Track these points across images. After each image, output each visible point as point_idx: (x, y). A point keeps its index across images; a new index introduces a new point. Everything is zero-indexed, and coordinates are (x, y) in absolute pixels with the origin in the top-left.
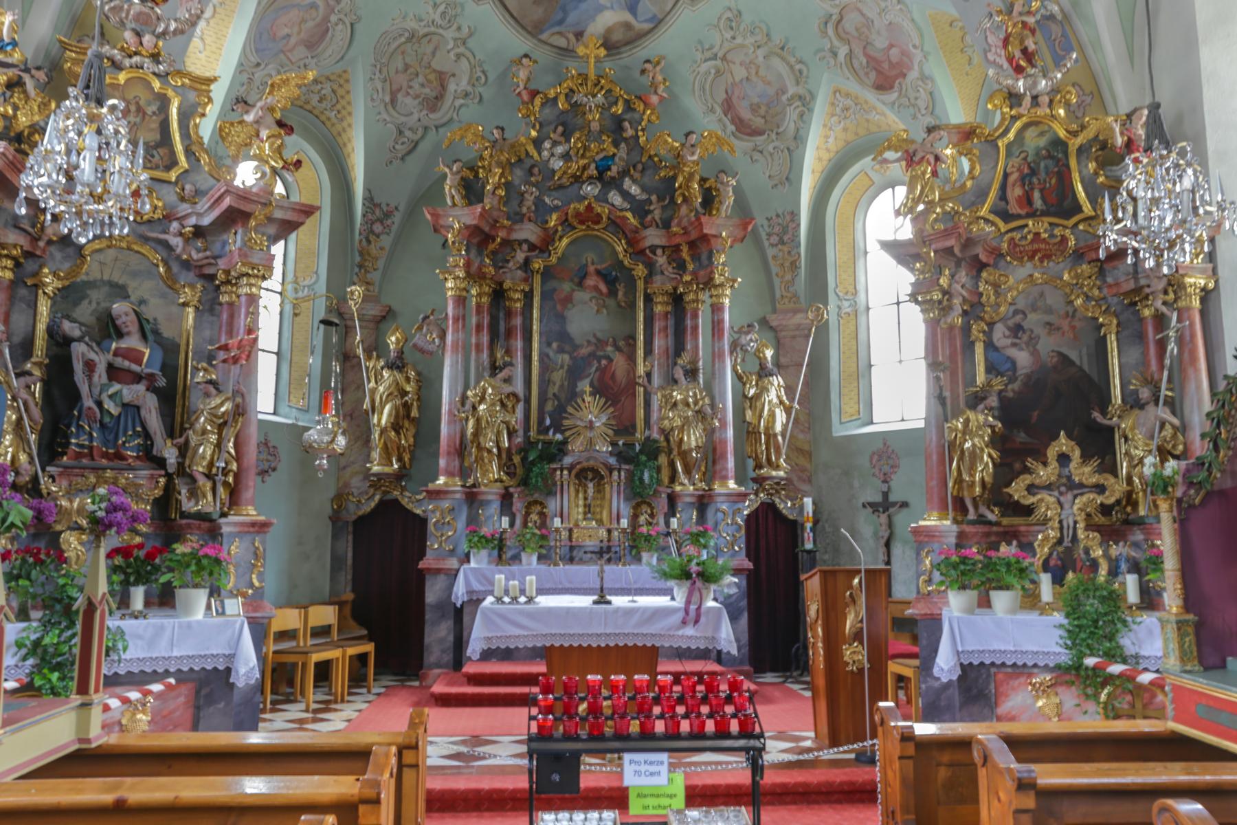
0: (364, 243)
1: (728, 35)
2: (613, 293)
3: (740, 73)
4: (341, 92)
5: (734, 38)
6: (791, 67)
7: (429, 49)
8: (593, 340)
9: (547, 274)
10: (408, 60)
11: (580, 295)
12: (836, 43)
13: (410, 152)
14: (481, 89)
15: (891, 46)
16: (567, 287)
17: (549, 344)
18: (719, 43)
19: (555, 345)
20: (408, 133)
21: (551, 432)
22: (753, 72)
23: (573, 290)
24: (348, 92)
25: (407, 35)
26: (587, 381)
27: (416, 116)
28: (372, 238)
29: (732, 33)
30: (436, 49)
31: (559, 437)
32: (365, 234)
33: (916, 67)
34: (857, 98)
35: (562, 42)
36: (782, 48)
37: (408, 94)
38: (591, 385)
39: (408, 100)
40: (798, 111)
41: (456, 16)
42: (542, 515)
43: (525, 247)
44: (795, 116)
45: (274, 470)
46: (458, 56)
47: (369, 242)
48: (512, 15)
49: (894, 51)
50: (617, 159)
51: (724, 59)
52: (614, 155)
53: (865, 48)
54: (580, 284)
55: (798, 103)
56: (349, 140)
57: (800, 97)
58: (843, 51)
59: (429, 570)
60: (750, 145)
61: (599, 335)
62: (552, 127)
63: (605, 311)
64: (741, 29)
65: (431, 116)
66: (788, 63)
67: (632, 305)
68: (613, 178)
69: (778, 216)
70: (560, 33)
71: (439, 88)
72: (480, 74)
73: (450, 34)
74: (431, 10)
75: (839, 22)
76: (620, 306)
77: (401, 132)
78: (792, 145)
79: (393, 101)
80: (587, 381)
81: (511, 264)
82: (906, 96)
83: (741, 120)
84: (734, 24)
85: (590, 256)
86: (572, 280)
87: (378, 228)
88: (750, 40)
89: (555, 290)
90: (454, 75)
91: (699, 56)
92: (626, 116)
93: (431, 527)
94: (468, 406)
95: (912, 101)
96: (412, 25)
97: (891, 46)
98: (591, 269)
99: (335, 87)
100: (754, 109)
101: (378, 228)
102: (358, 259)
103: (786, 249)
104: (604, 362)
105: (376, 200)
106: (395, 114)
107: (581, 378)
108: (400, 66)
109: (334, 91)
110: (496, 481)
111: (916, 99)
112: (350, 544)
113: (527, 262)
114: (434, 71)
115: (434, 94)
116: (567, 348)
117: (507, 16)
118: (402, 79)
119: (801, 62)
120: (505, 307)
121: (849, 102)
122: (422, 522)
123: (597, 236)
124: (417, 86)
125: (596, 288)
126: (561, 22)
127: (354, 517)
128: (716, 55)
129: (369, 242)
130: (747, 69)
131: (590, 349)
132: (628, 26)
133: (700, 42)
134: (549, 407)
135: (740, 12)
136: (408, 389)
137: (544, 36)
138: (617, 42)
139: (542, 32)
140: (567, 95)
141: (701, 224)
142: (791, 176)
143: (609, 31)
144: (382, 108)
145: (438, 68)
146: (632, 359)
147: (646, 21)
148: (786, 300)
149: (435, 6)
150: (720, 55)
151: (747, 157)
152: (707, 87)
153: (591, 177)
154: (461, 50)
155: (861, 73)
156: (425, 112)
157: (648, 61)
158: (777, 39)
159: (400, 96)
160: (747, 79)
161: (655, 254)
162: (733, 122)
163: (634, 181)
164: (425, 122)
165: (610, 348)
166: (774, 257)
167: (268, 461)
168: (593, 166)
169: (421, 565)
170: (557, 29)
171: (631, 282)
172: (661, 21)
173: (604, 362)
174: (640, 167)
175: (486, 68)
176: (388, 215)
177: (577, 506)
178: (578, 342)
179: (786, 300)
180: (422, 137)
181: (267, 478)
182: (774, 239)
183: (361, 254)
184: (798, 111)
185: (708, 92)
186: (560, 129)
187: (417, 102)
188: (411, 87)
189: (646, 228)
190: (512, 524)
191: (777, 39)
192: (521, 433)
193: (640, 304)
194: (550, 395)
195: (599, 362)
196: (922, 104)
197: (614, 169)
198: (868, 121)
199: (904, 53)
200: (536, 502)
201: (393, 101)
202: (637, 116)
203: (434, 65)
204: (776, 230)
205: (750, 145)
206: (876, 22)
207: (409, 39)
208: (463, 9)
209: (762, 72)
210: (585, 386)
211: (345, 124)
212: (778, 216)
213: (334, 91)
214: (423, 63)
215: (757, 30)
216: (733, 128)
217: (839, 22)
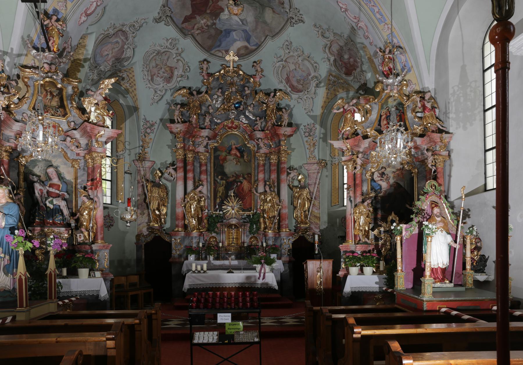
0: (143, 137)
1: (287, 51)
2: (242, 156)
3: (292, 67)
4: (131, 76)
5: (289, 53)
6: (312, 65)
7: (166, 58)
8: (235, 175)
9: (216, 149)
10: (157, 62)
11: (229, 157)
13: (160, 100)
14: (188, 74)
16: (224, 154)
17: (218, 177)
18: (284, 54)
19: (220, 177)
20: (159, 92)
23: (227, 155)
24: (134, 76)
25: (156, 52)
27: (162, 85)
39: (158, 79)
40: (315, 82)
43: (207, 139)
44: (314, 85)
46: (178, 60)
47: (145, 136)
50: (242, 103)
51: (286, 61)
57: (316, 77)
60: (297, 96)
61: (237, 173)
62: (217, 90)
64: (292, 49)
65: (168, 85)
68: (241, 111)
69: (308, 125)
70: (218, 50)
72: (187, 67)
73: (174, 51)
76: (245, 162)
77: (156, 92)
78: (313, 96)
79: (152, 79)
83: (293, 86)
87: (148, 131)
88: (296, 54)
89: (219, 155)
90: (176, 68)
91: (275, 60)
92: (247, 85)
96: (159, 48)
98: (234, 147)
99: (128, 74)
100: (298, 81)
101: (148, 131)
102: (141, 143)
104: (239, 183)
105: (148, 120)
106: (153, 85)
108: (154, 65)
109: (128, 76)
116: (225, 178)
117: (197, 44)
118: (155, 70)
120: (200, 162)
123: (236, 134)
125: (236, 155)
128: (282, 59)
129: (145, 136)
133: (276, 54)
138: (242, 54)
140: (222, 77)
141: (275, 130)
143: (239, 50)
145: (170, 66)
147: (254, 45)
149: (167, 40)
151: (296, 101)
152: (279, 72)
154: (179, 58)
157: (255, 62)
162: (290, 87)
163: (250, 112)
164: (166, 87)
165: (241, 178)
166: (307, 141)
168: (233, 106)
172: (260, 45)
173: (239, 183)
174: (252, 106)
175: (189, 65)
176: (152, 125)
178: (229, 176)
179: (311, 159)
180: (165, 94)
182: (307, 134)
183: (142, 141)
184: (315, 82)
185: (280, 75)
187: (162, 79)
189: (255, 131)
197: (242, 107)
201: (152, 79)
202: (251, 85)
205: (297, 96)
207: (157, 54)
208: (179, 41)
209: (301, 67)
212: (308, 125)
213: (128, 76)
216: (290, 89)
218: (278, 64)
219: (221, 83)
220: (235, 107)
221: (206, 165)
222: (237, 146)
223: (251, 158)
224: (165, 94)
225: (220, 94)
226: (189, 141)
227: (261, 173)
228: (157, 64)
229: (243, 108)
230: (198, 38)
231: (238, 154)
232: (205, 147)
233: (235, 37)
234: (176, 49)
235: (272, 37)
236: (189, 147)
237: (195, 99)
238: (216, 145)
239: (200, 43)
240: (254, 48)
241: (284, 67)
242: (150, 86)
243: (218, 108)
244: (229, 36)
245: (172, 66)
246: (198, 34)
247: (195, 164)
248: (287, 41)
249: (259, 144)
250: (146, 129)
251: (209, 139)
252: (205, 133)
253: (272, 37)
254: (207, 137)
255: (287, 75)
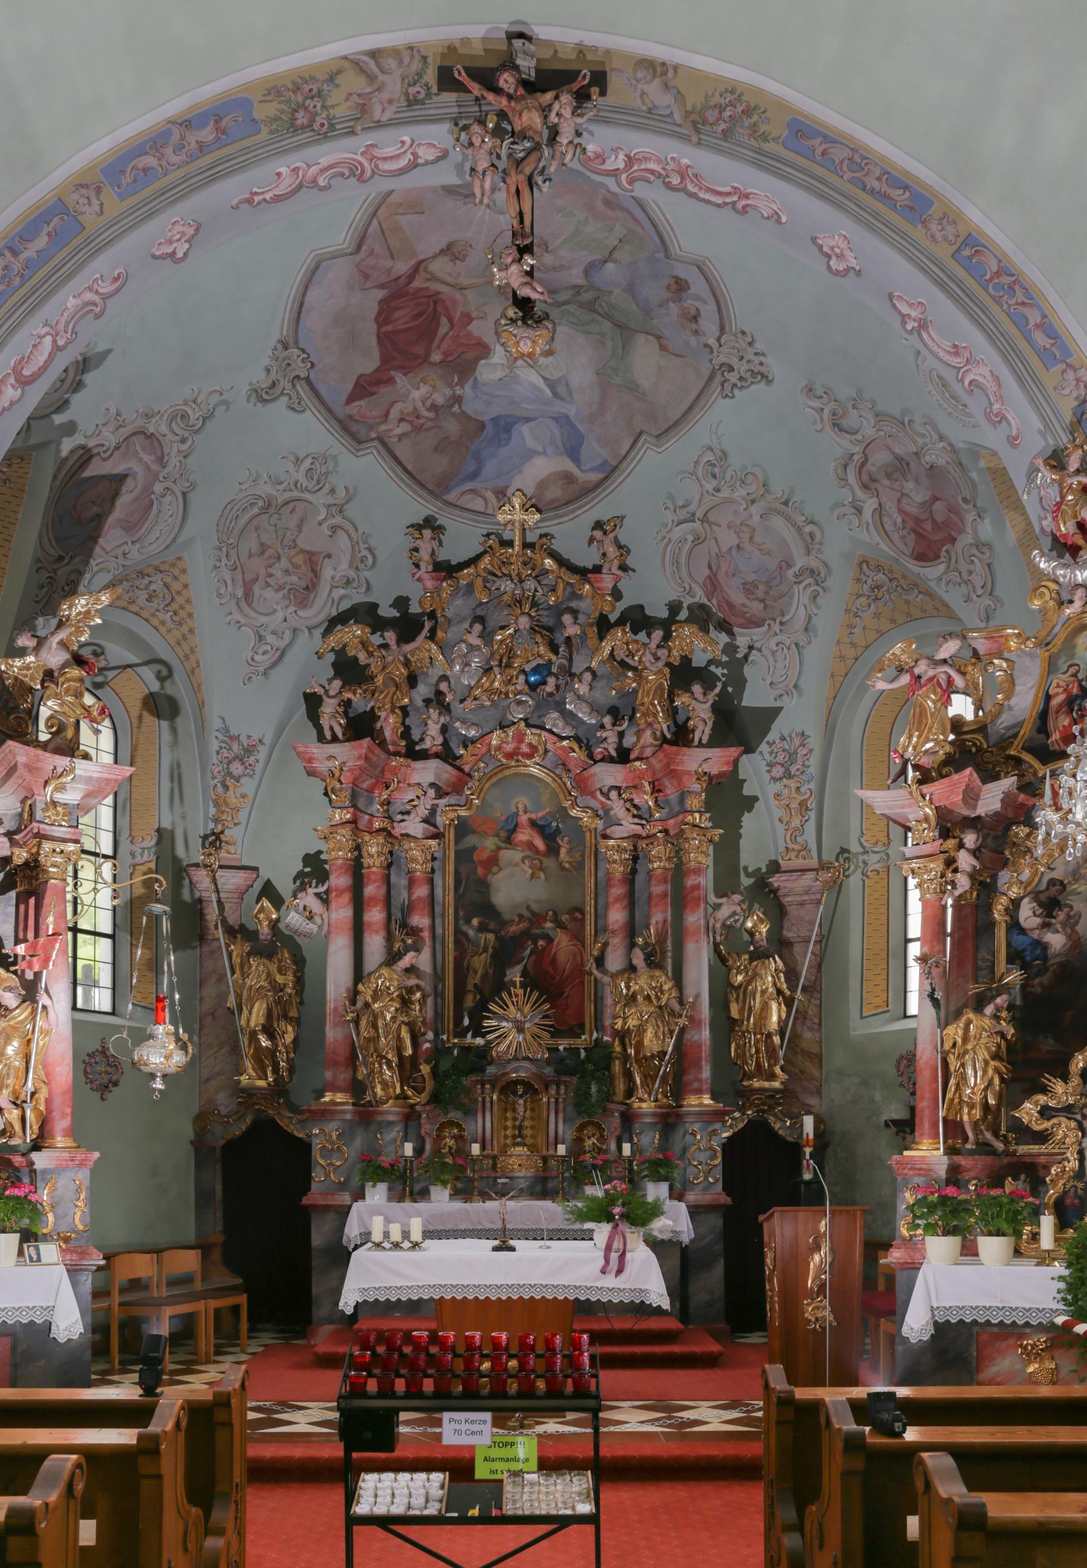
0: (220, 789)
1: (710, 486)
2: (553, 850)
3: (728, 539)
5: (718, 490)
6: (799, 529)
7: (292, 521)
8: (526, 914)
9: (462, 828)
10: (265, 538)
11: (508, 855)
12: (860, 494)
13: (274, 665)
14: (368, 574)
15: (935, 499)
17: (468, 921)
18: (697, 497)
19: (475, 922)
20: (270, 638)
21: (469, 1035)
22: (746, 537)
23: (499, 848)
24: (186, 586)
25: (260, 503)
26: (519, 968)
27: (280, 615)
28: (230, 782)
29: (715, 483)
30: (302, 521)
31: (479, 1041)
32: (220, 778)
33: (969, 529)
34: (891, 571)
35: (478, 504)
36: (786, 503)
37: (268, 585)
38: (524, 973)
39: (269, 593)
40: (809, 591)
41: (327, 473)
42: (459, 1138)
43: (431, 793)
44: (805, 599)
45: (116, 1084)
46: (334, 529)
47: (226, 787)
48: (405, 469)
49: (938, 506)
51: (704, 519)
52: (550, 662)
53: (899, 501)
54: (509, 840)
55: (809, 580)
56: (192, 651)
57: (812, 572)
58: (870, 505)
59: (315, 1207)
61: (535, 907)
62: (466, 625)
63: (542, 876)
64: (728, 476)
65: (301, 613)
66: (794, 525)
67: (580, 866)
68: (551, 695)
69: (783, 738)
71: (311, 574)
72: (365, 553)
73: (320, 500)
74: (292, 469)
75: (863, 464)
76: (563, 869)
77: (261, 638)
78: (802, 640)
79: (248, 596)
80: (519, 968)
81: (413, 815)
82: (957, 570)
84: (716, 470)
85: (521, 802)
86: (498, 835)
87: (237, 768)
89: (474, 849)
90: (329, 556)
91: (669, 516)
93: (316, 1153)
94: (359, 1004)
95: (965, 577)
97: (935, 499)
98: (524, 819)
100: (749, 589)
101: (237, 768)
102: (212, 811)
103: (793, 784)
104: (541, 943)
105: (234, 732)
106: (252, 614)
107: (511, 965)
108: (255, 547)
110: (397, 1097)
111: (970, 573)
112: (219, 1174)
113: (433, 810)
114: (302, 551)
115: (304, 584)
116: (492, 925)
117: (398, 470)
118: (258, 566)
119: (811, 522)
121: (880, 577)
122: (304, 1148)
124: (279, 574)
125: (530, 845)
126: (474, 476)
127: (222, 1142)
128: (693, 515)
129: (226, 787)
130: (737, 533)
131: (523, 926)
132: (568, 478)
133: (670, 497)
134: (469, 1001)
135: (724, 453)
136: (280, 979)
137: (451, 497)
138: (554, 501)
139: (448, 490)
142: (800, 683)
143: (542, 485)
144: (234, 609)
145: (308, 548)
146: (578, 938)
147: (593, 469)
148: (793, 855)
149: (298, 461)
150: (699, 514)
152: (683, 560)
153: (520, 692)
154: (338, 520)
155: (895, 537)
156: (292, 609)
158: (778, 489)
159: (256, 588)
160: (738, 546)
161: (609, 799)
164: (293, 622)
165: (549, 925)
166: (777, 796)
167: (107, 1073)
168: (522, 678)
169: (306, 1201)
170: (469, 486)
171: (578, 830)
172: (616, 468)
173: (541, 943)
174: (588, 676)
175: (373, 543)
176: (249, 750)
177: (506, 1128)
178: (506, 917)
180: (290, 644)
181: (107, 1095)
182: (778, 771)
183: (216, 804)
184: (809, 591)
185: (683, 568)
186: (478, 627)
187: (280, 595)
188: (271, 575)
190: (419, 1151)
191: (778, 489)
192: (430, 1035)
193: (589, 864)
194: (470, 987)
195: (535, 943)
196: (978, 581)
197: (551, 681)
198: (907, 602)
199: (952, 509)
200: (452, 1124)
201: (248, 596)
203: (302, 543)
204: (780, 758)
206: (913, 466)
207: (265, 510)
208: (336, 465)
209: (756, 539)
210: (515, 975)
211: (185, 629)
212: (783, 738)
214: (285, 542)
215: (750, 478)
217: (863, 464)
218: (678, 532)
219: (481, 604)
220: (527, 682)
221: (431, 882)
222: (533, 816)
223: (583, 856)
224: (290, 644)
225: (477, 642)
226: (370, 801)
227: (617, 906)
228: (262, 544)
229: (557, 687)
230: (403, 451)
231: (540, 844)
232: (425, 821)
233: (530, 443)
234: (326, 490)
235: (658, 437)
236: (370, 822)
237: (390, 658)
238: (463, 813)
239: (410, 467)
240: (595, 477)
241: (698, 540)
242: (242, 621)
243: (471, 688)
244: (509, 439)
245: (315, 549)
246: (400, 438)
247: (393, 878)
248: (712, 450)
249: (612, 809)
250: (230, 762)
251: (440, 793)
252: (426, 772)
253: (658, 437)
254: (432, 785)
255: (710, 567)
